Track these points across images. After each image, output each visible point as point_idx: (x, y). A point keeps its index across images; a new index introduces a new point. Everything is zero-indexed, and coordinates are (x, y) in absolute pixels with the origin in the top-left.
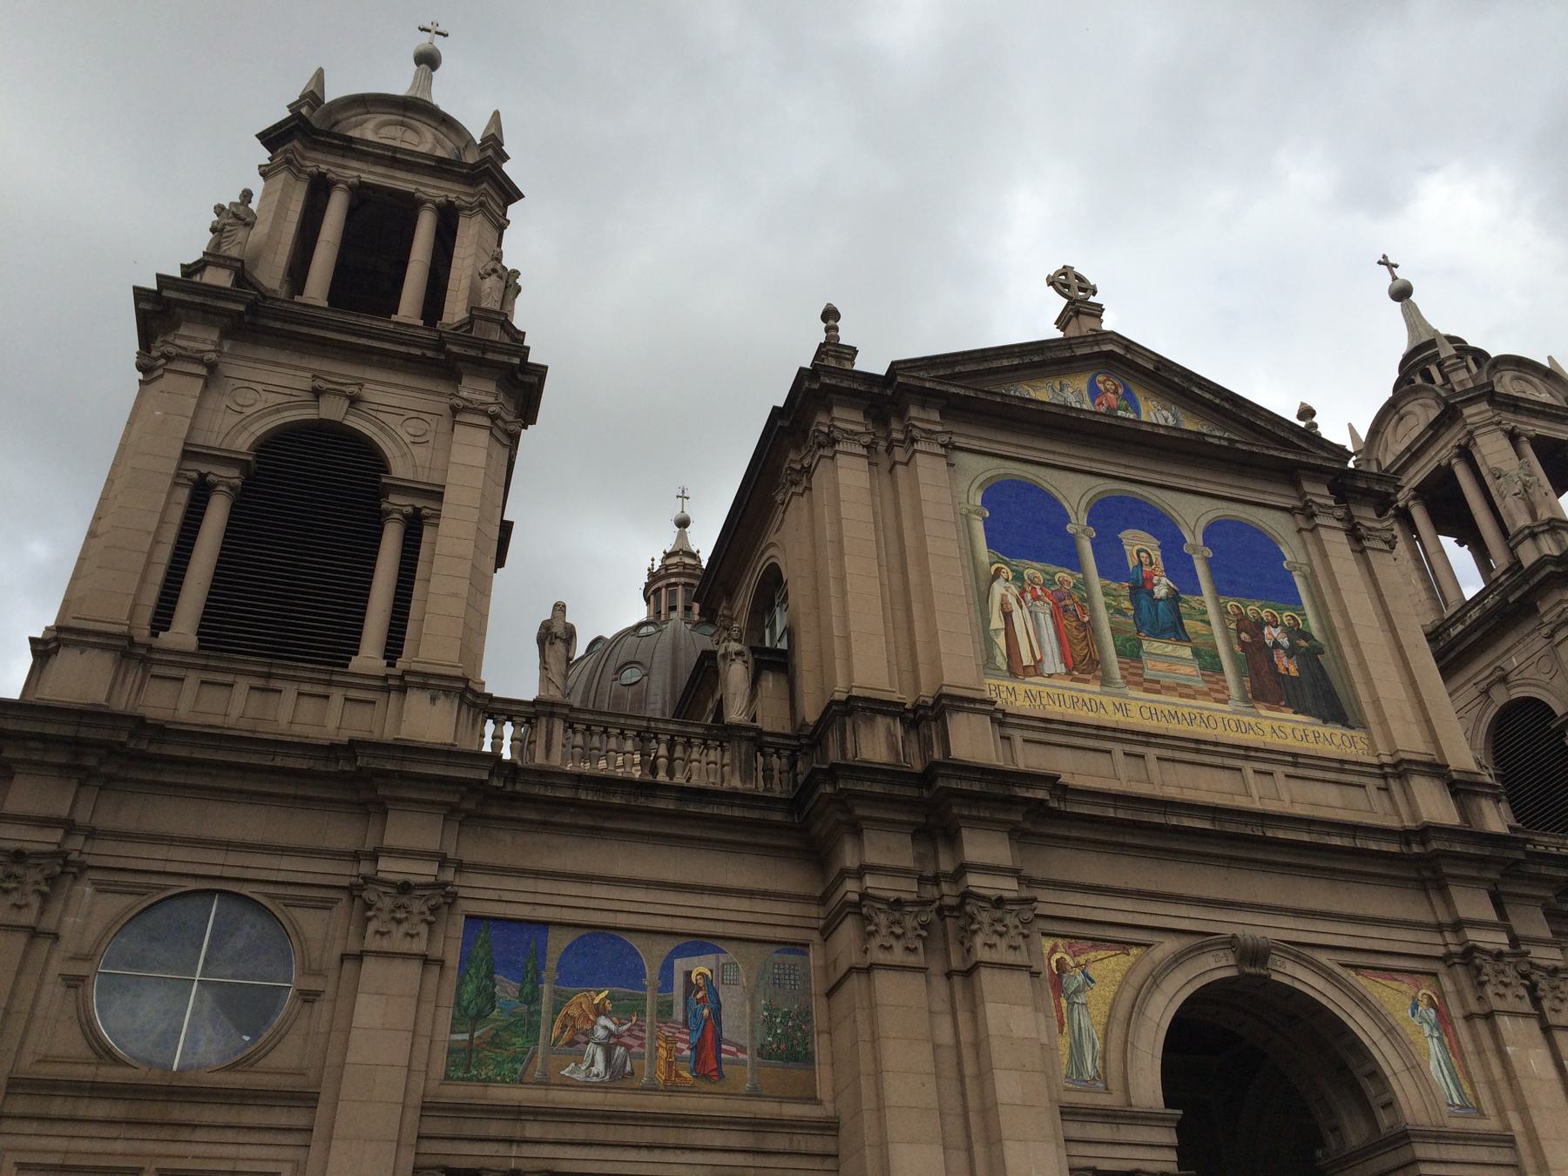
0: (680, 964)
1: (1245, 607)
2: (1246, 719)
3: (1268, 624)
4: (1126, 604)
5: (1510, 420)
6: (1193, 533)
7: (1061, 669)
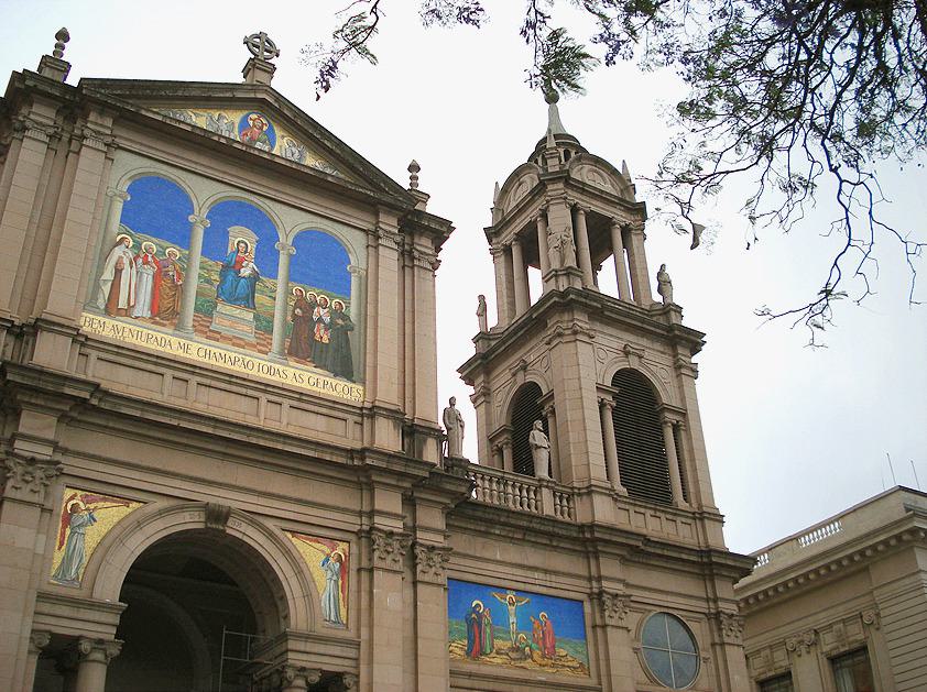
2: (277, 366)
4: (216, 277)
5: (574, 197)
7: (148, 314)
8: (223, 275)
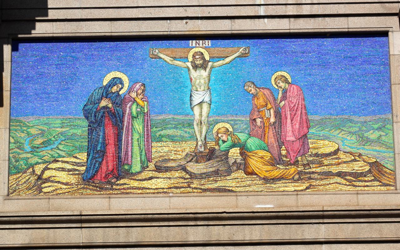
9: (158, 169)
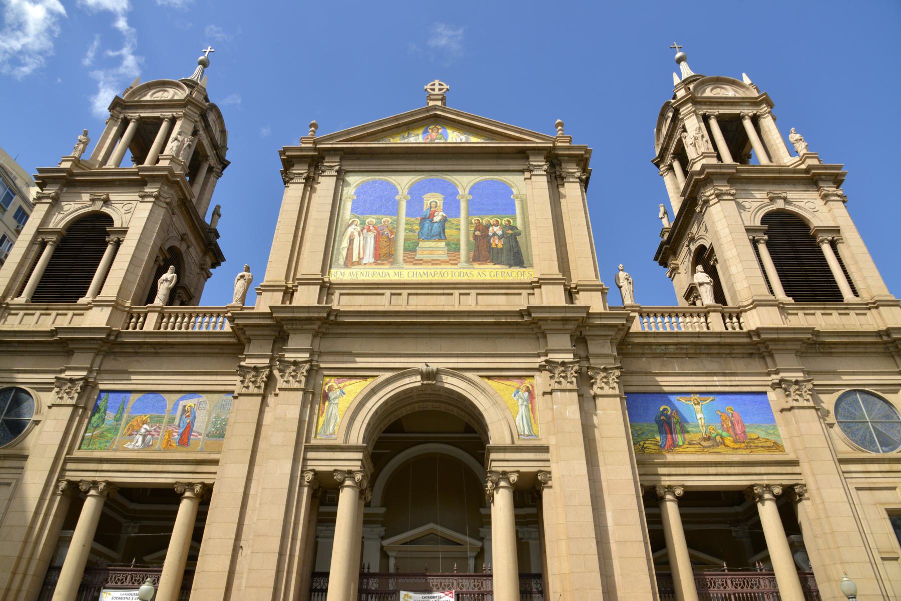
0: (182, 403)
1: (482, 219)
2: (465, 271)
3: (494, 225)
4: (417, 227)
6: (464, 190)
7: (372, 260)
8: (422, 224)
9: (690, 444)
